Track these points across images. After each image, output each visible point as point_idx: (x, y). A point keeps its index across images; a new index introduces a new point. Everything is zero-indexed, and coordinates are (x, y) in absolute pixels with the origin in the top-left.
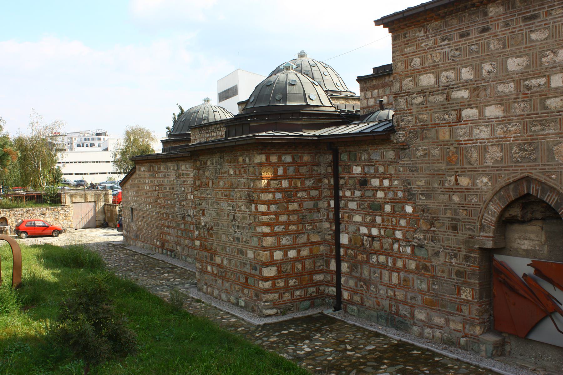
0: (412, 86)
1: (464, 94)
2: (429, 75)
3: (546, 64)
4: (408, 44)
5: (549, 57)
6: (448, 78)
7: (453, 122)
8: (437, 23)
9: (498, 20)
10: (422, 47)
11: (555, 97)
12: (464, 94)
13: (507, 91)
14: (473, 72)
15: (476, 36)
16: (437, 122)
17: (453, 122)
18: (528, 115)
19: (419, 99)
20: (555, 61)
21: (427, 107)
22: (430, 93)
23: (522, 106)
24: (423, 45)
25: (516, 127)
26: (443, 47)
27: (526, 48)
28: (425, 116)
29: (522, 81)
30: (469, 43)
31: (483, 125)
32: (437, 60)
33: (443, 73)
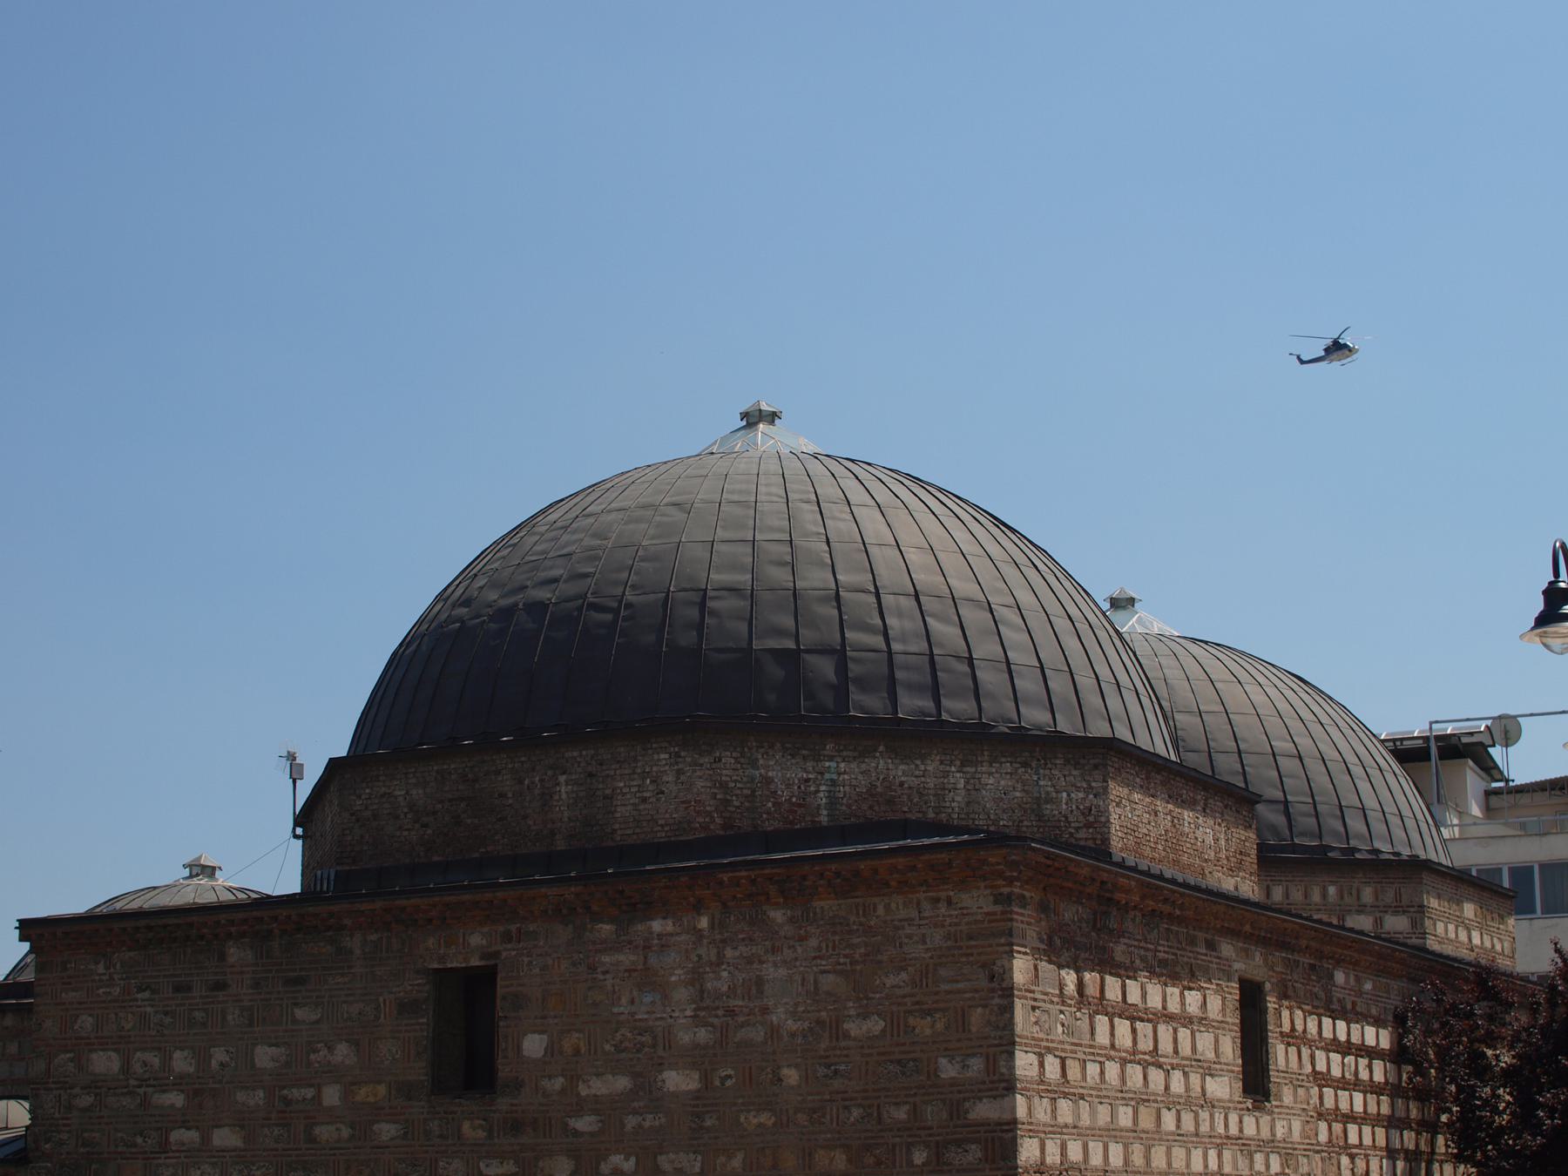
0: (73, 1070)
1: (176, 1099)
2: (110, 1053)
3: (317, 1065)
4: (70, 983)
5: (321, 1053)
6: (146, 1066)
7: (152, 1153)
8: (132, 954)
9: (242, 973)
10: (98, 995)
11: (327, 1123)
12: (176, 1099)
13: (252, 1103)
14: (193, 1061)
15: (204, 994)
16: (120, 1149)
17: (152, 1153)
18: (284, 1150)
19: (87, 1100)
20: (329, 1062)
21: (102, 1117)
22: (109, 1089)
23: (276, 1132)
24: (101, 991)
25: (264, 1169)
26: (139, 1003)
27: (286, 1031)
28: (97, 1135)
29: (277, 1089)
30: (190, 1005)
31: (207, 1163)
32: (128, 1026)
33: (139, 1054)
